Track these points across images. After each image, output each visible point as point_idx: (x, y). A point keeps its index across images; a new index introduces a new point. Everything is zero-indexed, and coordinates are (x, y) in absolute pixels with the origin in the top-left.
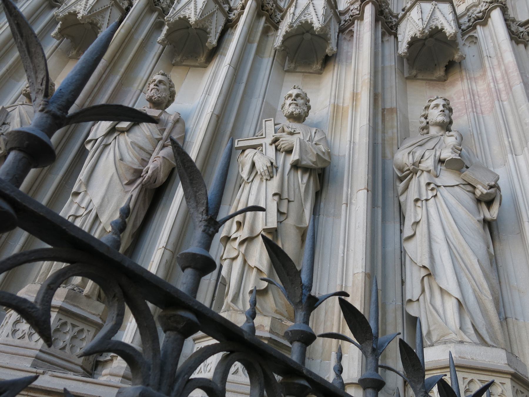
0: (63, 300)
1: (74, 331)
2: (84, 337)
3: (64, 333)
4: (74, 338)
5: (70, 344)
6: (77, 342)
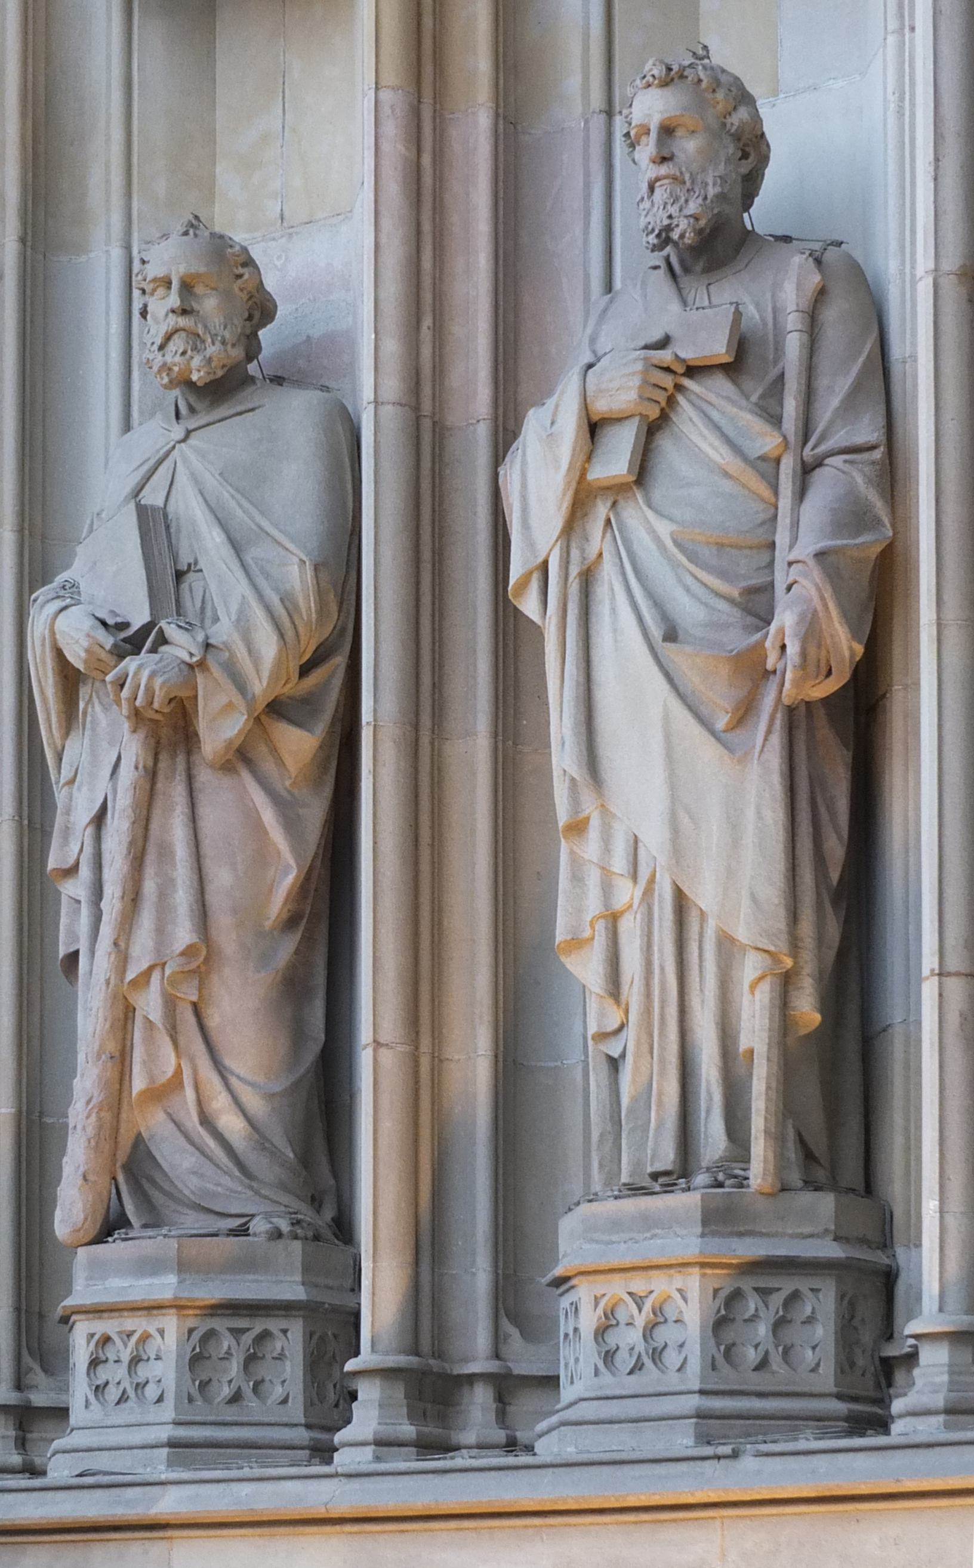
0: (699, 1230)
1: (772, 1309)
2: (808, 1310)
3: (746, 1321)
4: (779, 1325)
5: (777, 1346)
6: (794, 1334)
